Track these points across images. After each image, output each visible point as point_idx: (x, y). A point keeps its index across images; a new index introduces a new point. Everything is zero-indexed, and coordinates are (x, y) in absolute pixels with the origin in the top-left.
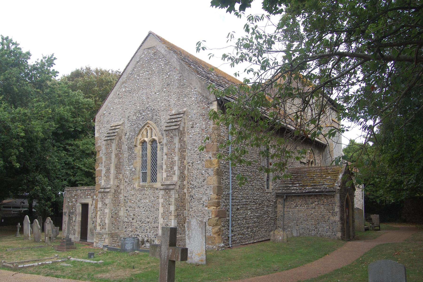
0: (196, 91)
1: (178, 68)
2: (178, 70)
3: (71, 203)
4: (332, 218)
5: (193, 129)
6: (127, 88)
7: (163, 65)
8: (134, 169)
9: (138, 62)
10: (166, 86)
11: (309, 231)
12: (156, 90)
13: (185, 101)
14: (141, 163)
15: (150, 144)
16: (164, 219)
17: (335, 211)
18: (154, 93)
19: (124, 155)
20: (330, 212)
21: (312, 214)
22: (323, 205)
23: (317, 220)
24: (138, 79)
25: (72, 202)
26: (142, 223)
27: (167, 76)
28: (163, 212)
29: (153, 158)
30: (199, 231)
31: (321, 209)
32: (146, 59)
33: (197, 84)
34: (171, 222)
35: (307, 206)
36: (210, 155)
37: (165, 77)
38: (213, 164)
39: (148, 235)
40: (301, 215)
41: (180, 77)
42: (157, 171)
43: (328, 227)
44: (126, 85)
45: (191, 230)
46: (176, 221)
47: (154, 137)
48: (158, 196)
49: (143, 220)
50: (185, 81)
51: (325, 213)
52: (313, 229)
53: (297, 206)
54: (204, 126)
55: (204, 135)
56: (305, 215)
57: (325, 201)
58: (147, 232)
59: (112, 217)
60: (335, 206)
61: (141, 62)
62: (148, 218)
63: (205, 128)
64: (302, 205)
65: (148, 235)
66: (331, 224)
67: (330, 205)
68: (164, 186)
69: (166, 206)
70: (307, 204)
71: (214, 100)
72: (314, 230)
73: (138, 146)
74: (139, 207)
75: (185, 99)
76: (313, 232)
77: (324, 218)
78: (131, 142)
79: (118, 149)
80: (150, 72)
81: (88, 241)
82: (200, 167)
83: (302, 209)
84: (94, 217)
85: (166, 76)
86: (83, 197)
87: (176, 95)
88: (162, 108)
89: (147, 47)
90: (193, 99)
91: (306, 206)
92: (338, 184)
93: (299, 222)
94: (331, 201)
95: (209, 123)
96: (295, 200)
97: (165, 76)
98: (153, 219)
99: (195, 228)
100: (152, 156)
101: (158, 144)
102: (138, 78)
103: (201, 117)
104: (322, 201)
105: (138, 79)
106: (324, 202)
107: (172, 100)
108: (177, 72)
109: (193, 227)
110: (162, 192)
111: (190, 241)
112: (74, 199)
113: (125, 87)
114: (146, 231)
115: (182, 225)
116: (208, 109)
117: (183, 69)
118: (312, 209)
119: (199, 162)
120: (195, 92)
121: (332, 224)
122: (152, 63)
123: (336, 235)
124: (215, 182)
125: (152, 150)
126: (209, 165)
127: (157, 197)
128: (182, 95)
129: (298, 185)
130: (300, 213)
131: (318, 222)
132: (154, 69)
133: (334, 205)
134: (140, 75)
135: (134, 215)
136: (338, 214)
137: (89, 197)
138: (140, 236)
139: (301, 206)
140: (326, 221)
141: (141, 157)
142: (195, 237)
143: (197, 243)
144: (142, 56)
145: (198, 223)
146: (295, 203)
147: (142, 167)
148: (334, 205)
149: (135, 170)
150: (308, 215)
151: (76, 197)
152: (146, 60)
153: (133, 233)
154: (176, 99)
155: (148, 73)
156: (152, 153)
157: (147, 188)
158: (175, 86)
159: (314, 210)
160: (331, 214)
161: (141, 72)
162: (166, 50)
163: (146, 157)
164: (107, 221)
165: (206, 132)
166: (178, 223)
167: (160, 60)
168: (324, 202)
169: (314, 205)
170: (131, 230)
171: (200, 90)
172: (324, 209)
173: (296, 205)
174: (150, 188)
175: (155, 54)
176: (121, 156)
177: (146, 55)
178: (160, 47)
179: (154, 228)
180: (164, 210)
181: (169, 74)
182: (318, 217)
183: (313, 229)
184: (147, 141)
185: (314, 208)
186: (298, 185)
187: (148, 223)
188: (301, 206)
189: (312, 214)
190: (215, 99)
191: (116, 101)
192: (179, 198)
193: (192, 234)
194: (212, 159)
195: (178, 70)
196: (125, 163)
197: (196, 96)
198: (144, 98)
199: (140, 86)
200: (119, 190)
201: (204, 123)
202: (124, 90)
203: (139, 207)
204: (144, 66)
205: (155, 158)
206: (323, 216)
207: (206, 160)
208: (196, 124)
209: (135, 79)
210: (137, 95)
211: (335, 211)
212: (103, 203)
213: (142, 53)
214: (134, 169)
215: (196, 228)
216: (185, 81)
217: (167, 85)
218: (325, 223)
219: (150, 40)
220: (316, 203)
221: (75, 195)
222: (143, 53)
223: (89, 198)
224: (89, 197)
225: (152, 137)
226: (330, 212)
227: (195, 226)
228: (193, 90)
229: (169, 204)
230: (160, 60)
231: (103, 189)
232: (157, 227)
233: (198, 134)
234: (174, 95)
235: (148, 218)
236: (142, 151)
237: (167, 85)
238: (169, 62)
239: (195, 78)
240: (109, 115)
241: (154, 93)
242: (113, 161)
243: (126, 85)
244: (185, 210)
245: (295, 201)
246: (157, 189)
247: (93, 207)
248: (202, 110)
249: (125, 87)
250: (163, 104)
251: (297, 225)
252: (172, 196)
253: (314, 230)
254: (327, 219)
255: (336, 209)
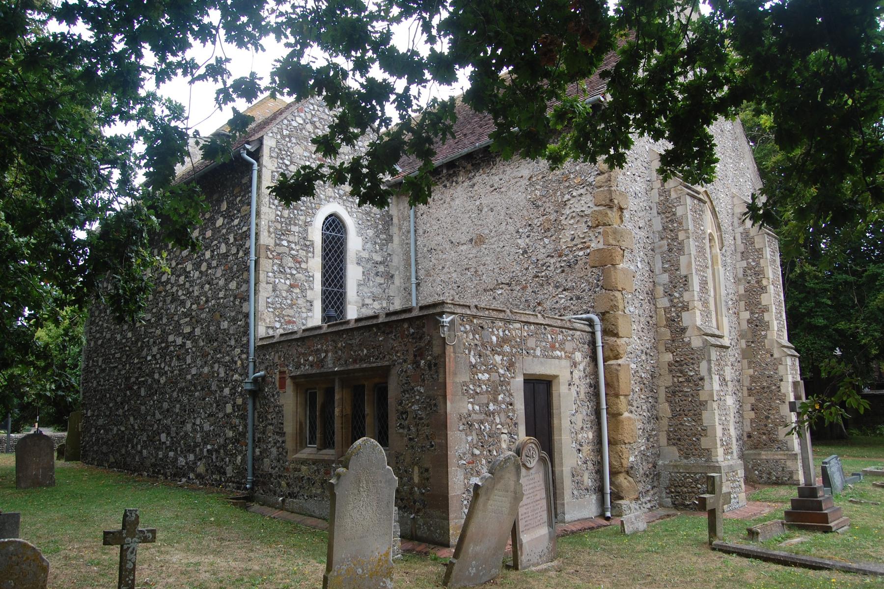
3: (485, 371)
25: (491, 369)
81: (568, 517)
84: (582, 428)
86: (538, 353)
112: (498, 358)
137: (558, 353)
221: (504, 340)
223: (558, 358)
224: (558, 353)
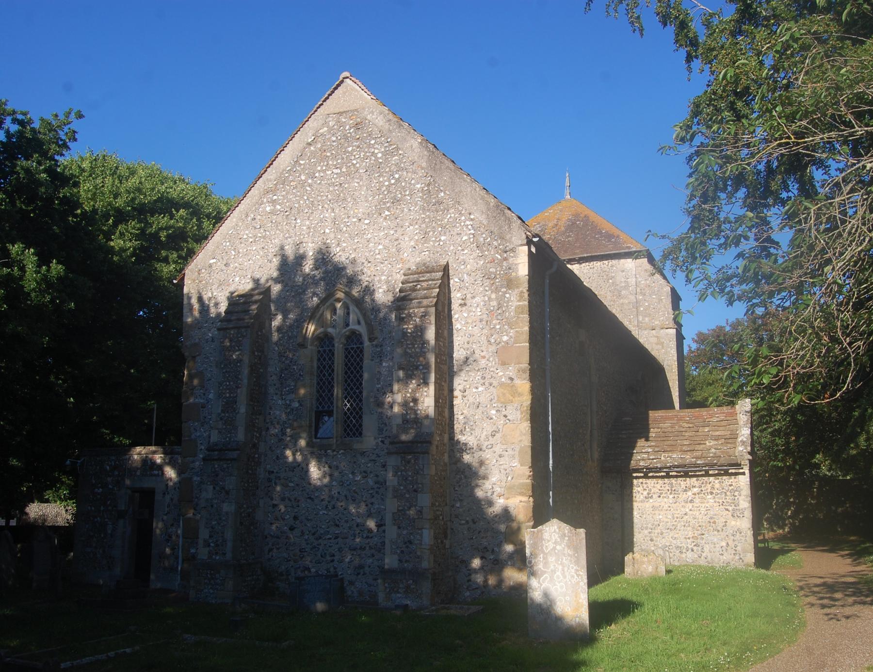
0: (472, 220)
1: (424, 165)
2: (422, 168)
4: (733, 523)
5: (464, 308)
6: (279, 204)
7: (380, 155)
8: (296, 405)
9: (309, 144)
10: (388, 205)
11: (681, 552)
12: (361, 210)
13: (441, 243)
14: (315, 390)
15: (342, 343)
16: (399, 528)
17: (741, 507)
18: (355, 220)
19: (269, 369)
20: (727, 510)
21: (686, 514)
22: (712, 493)
23: (699, 528)
24: (310, 185)
26: (317, 539)
27: (393, 181)
28: (398, 510)
29: (349, 377)
30: (569, 555)
31: (708, 502)
32: (334, 139)
33: (476, 204)
34: (421, 535)
35: (674, 497)
36: (511, 371)
37: (387, 183)
38: (520, 395)
39: (335, 568)
40: (661, 517)
41: (429, 185)
42: (361, 409)
43: (724, 544)
44: (275, 197)
45: (543, 552)
46: (432, 531)
47: (353, 326)
48: (365, 472)
49: (322, 532)
50: (442, 194)
51: (715, 512)
52: (690, 547)
53: (651, 497)
54: (494, 303)
55: (495, 325)
56: (670, 517)
57: (717, 486)
58: (333, 561)
59: (241, 524)
60: (740, 495)
61: (319, 146)
62: (337, 526)
63: (496, 308)
64: (661, 494)
65: (335, 568)
66: (730, 535)
67: (728, 493)
68: (397, 446)
69: (407, 496)
70: (672, 491)
71: (520, 242)
72: (692, 550)
73: (309, 347)
74: (310, 498)
75: (443, 238)
76: (690, 554)
77: (714, 523)
78: (290, 338)
79: (256, 353)
80: (344, 170)
82: (483, 399)
83: (663, 504)
85: (389, 181)
87: (417, 227)
88: (378, 256)
89: (337, 111)
90: (465, 238)
91: (671, 496)
92: (746, 449)
93: (656, 531)
94: (731, 485)
95: (507, 295)
96: (646, 483)
97: (386, 181)
98: (350, 528)
99: (554, 548)
100: (346, 373)
101: (367, 343)
102: (310, 181)
103: (487, 283)
104: (709, 486)
105: (310, 185)
106: (713, 488)
107: (407, 239)
108: (421, 173)
109: (551, 545)
110: (393, 461)
111: (539, 582)
113: (274, 202)
114: (329, 558)
115: (442, 542)
116: (505, 263)
117: (438, 167)
118: (687, 502)
119: (480, 389)
120: (468, 223)
121: (733, 535)
122: (350, 149)
123: (743, 561)
124: (524, 437)
125: (346, 357)
126: (507, 395)
127: (364, 474)
128: (434, 227)
129: (650, 450)
130: (657, 512)
131: (699, 532)
132: (355, 162)
133: (736, 493)
134: (317, 175)
135: (295, 518)
136: (745, 513)
138: (313, 570)
139: (659, 497)
140: (719, 528)
141: (315, 373)
142: (554, 572)
143: (562, 587)
144: (321, 131)
145: (565, 535)
146: (645, 490)
147: (318, 400)
148: (736, 493)
149: (301, 405)
150: (675, 516)
151: (116, 473)
152: (334, 141)
153: (292, 563)
154: (416, 237)
155: (336, 171)
156: (346, 365)
157: (334, 451)
158: (416, 204)
159: (690, 505)
160: (730, 514)
161: (319, 168)
162: (389, 120)
163: (330, 375)
164: (229, 535)
165: (499, 317)
166: (436, 538)
167: (373, 142)
168: (713, 488)
169: (690, 493)
170: (285, 555)
171: (483, 219)
172: (715, 502)
173: (648, 494)
174: (342, 451)
175: (357, 126)
176: (262, 370)
177: (330, 129)
178: (372, 113)
179: (355, 549)
180: (399, 506)
181: (397, 176)
182: (700, 520)
183: (690, 547)
184: (334, 335)
185: (691, 501)
186: (650, 450)
187: (336, 538)
188: (659, 497)
189: (686, 514)
190: (525, 241)
191: (246, 234)
192: (437, 474)
193: (546, 564)
194: (517, 382)
195: (422, 168)
196: (271, 390)
197: (472, 232)
198: (327, 231)
199: (316, 202)
200: (257, 456)
201: (493, 296)
202: (268, 209)
203: (310, 498)
204: (328, 154)
205: (355, 377)
206: (711, 518)
207: (502, 385)
208: (473, 297)
209: (303, 184)
210: (307, 223)
211: (741, 507)
212: (217, 488)
213: (321, 122)
214: (296, 405)
215: (558, 547)
216: (442, 194)
217: (393, 203)
218: (716, 532)
219: (344, 93)
220: (696, 490)
222: (325, 123)
225: (348, 325)
226: (727, 510)
227: (556, 543)
228: (463, 218)
229: (415, 491)
230: (373, 142)
231: (216, 453)
232: (361, 548)
233: (478, 323)
234: (411, 227)
235: (337, 526)
236: (319, 360)
237: (393, 203)
238: (398, 149)
239: (469, 190)
240: (224, 268)
241: (355, 220)
242: (245, 381)
243: (275, 197)
244: (446, 505)
245: (645, 486)
246: (363, 454)
247: (168, 498)
248: (488, 265)
249: (274, 202)
250: (381, 247)
251: (652, 540)
252: (422, 470)
253: (692, 550)
254: (721, 525)
255: (741, 502)
